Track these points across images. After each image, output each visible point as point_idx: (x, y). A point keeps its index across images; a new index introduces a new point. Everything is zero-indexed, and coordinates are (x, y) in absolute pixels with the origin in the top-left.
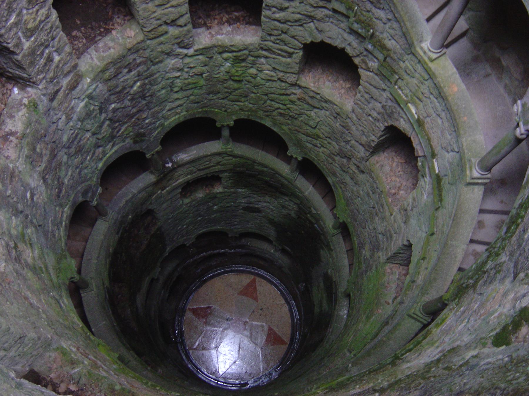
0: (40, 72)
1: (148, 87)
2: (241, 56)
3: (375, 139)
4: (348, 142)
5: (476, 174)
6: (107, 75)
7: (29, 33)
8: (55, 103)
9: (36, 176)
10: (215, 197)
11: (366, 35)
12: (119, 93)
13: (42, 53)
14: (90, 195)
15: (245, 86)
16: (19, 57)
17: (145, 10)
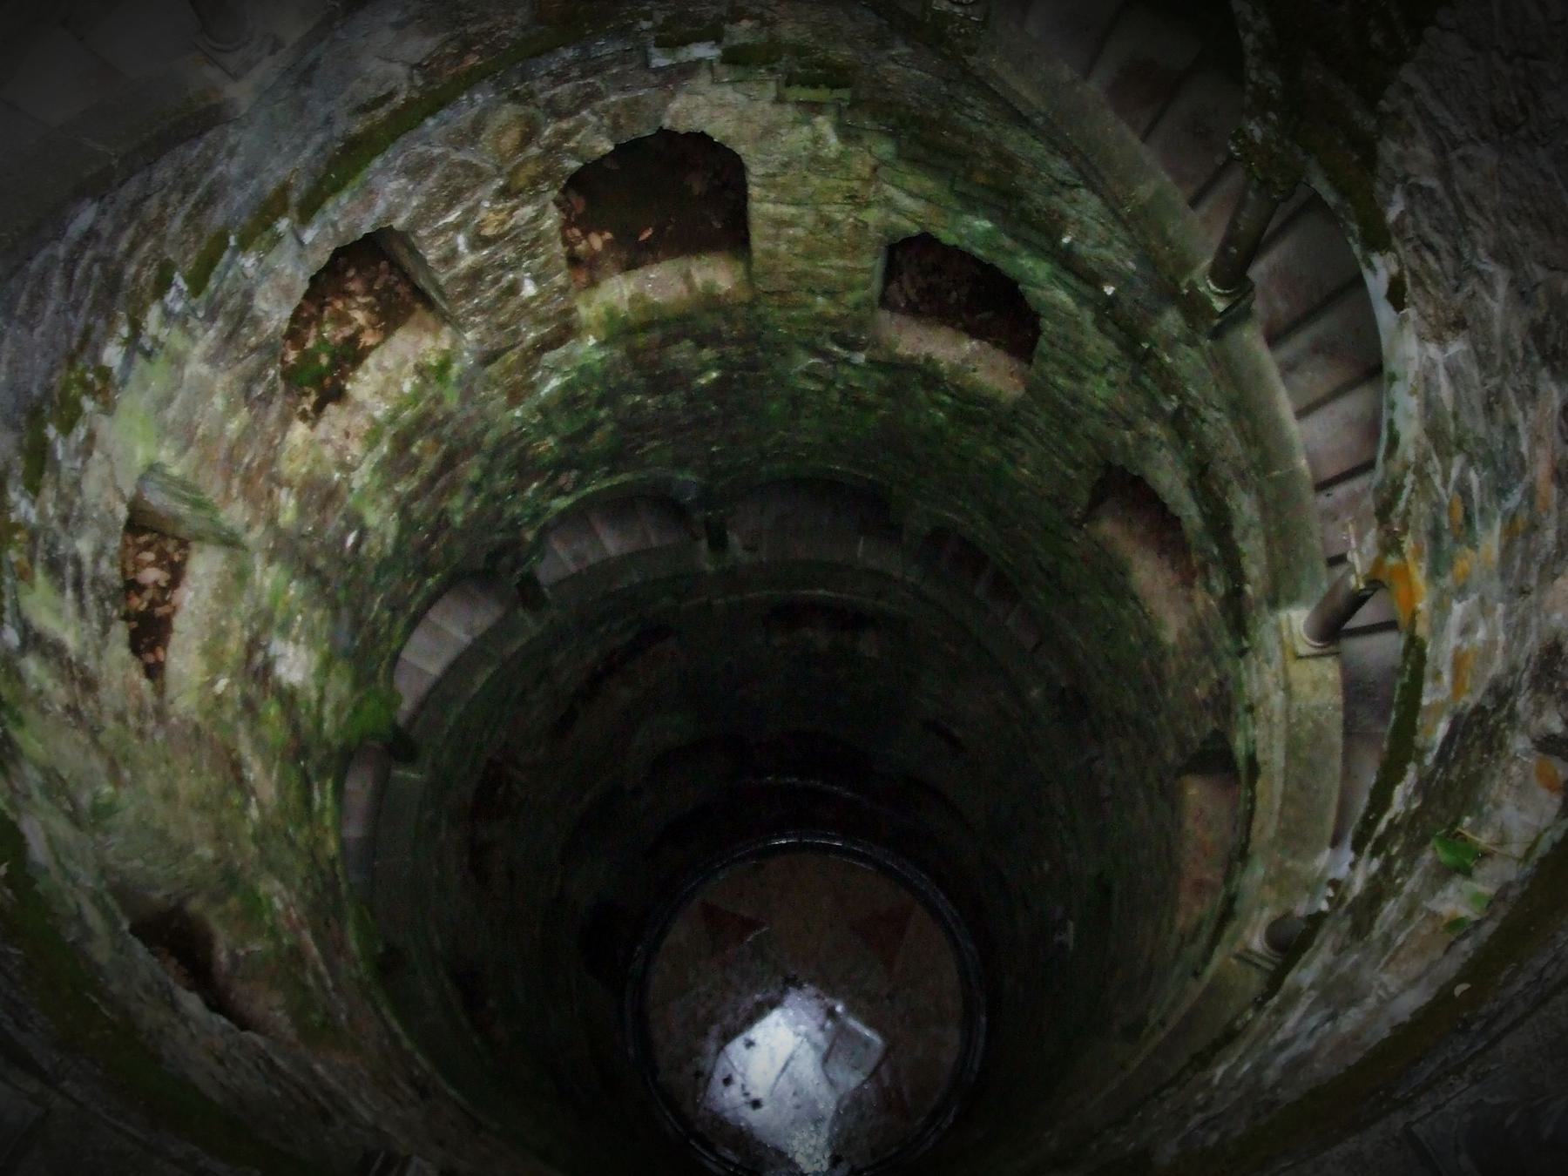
0: (479, 310)
1: (735, 386)
2: (973, 408)
6: (641, 340)
7: (479, 241)
8: (493, 369)
9: (386, 501)
11: (1220, 522)
12: (662, 380)
13: (496, 281)
14: (507, 560)
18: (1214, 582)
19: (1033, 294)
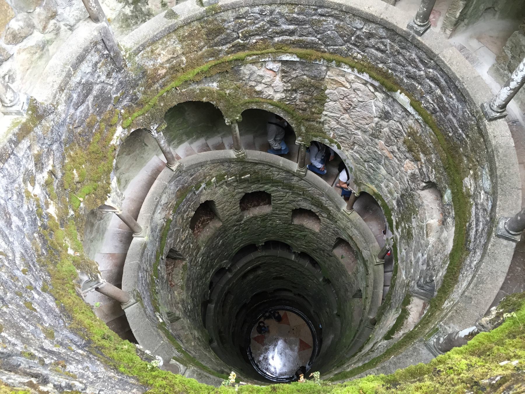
2: (264, 218)
3: (333, 243)
4: (321, 244)
5: (378, 261)
8: (192, 264)
10: (259, 276)
11: (319, 205)
15: (268, 229)
16: (180, 253)
17: (222, 214)
18: (323, 215)
19: (268, 192)
